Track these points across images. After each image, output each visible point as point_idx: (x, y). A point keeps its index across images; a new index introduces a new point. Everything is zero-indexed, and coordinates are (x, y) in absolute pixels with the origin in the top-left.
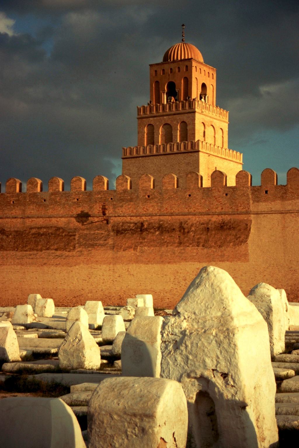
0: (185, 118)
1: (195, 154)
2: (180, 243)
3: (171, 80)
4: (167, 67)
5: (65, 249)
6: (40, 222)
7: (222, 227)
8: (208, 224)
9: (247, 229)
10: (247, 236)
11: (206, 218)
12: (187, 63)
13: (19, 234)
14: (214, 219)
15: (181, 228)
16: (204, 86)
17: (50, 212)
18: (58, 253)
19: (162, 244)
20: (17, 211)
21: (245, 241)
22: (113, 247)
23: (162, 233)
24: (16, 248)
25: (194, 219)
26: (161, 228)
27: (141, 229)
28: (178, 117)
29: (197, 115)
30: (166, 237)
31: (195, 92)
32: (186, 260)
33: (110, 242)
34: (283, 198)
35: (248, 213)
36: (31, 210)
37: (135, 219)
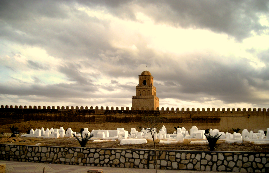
0: (149, 89)
1: (152, 99)
2: (206, 122)
3: (145, 80)
4: (143, 76)
5: (181, 123)
6: (175, 117)
8: (212, 118)
10: (220, 121)
11: (211, 117)
12: (149, 76)
13: (170, 119)
14: (213, 117)
17: (177, 115)
18: (179, 124)
19: (202, 122)
21: (220, 122)
23: (202, 120)
25: (209, 117)
28: (147, 89)
29: (153, 89)
32: (208, 125)
33: (191, 121)
35: (220, 116)
36: (173, 114)
37: (196, 117)
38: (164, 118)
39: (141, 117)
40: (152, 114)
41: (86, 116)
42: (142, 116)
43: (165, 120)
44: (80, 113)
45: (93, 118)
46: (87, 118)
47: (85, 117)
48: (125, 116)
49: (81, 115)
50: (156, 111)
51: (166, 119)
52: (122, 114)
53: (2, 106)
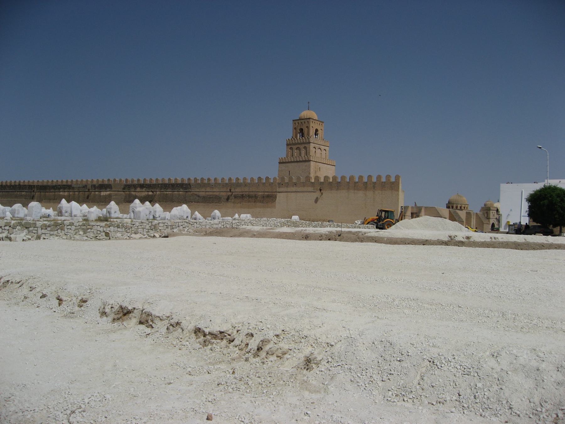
0: (306, 145)
7: (268, 196)
9: (276, 197)
13: (204, 197)
15: (255, 196)
16: (317, 130)
17: (215, 190)
19: (249, 202)
20: (203, 190)
22: (233, 202)
24: (202, 202)
26: (249, 196)
27: (242, 197)
30: (250, 199)
31: (312, 132)
34: (287, 187)
36: (208, 189)
38: (196, 195)
39: (167, 194)
40: (181, 190)
41: (103, 194)
42: (169, 192)
43: (197, 198)
44: (95, 189)
45: (110, 196)
46: (103, 196)
47: (100, 196)
48: (146, 193)
49: (97, 193)
50: (186, 184)
51: (199, 196)
52: (144, 190)
53: (2, 182)
